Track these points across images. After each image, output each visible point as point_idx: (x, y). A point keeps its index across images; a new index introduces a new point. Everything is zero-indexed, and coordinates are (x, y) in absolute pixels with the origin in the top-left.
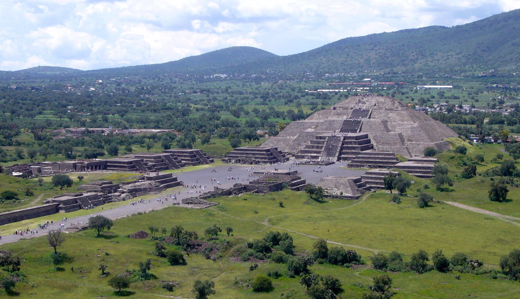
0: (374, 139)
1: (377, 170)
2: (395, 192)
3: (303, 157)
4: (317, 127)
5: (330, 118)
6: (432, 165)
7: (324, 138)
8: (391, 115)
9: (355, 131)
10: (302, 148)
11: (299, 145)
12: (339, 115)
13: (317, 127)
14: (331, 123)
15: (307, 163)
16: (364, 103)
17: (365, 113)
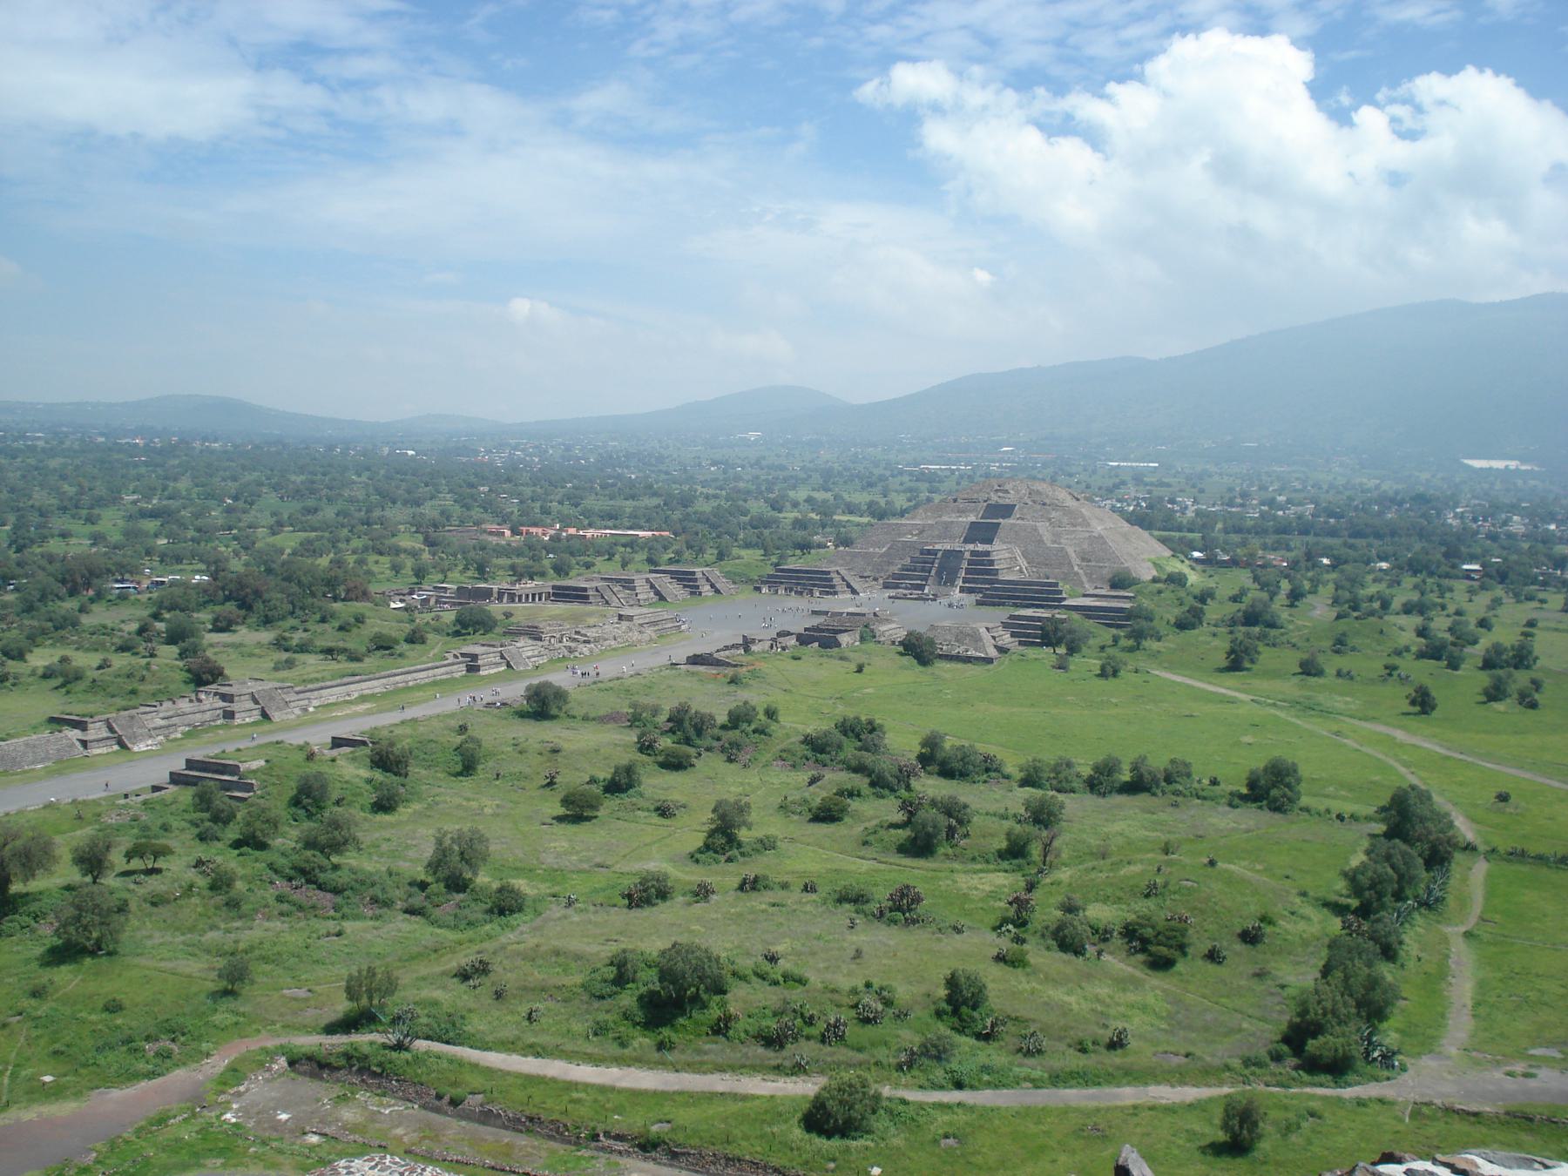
0: (1025, 554)
1: (1029, 612)
2: (1062, 650)
3: (897, 587)
4: (921, 532)
5: (945, 518)
6: (1128, 606)
7: (935, 552)
8: (1054, 514)
9: (990, 541)
10: (895, 569)
11: (890, 563)
12: (962, 512)
13: (921, 532)
14: (947, 525)
15: (904, 597)
16: (1007, 492)
17: (1007, 510)
